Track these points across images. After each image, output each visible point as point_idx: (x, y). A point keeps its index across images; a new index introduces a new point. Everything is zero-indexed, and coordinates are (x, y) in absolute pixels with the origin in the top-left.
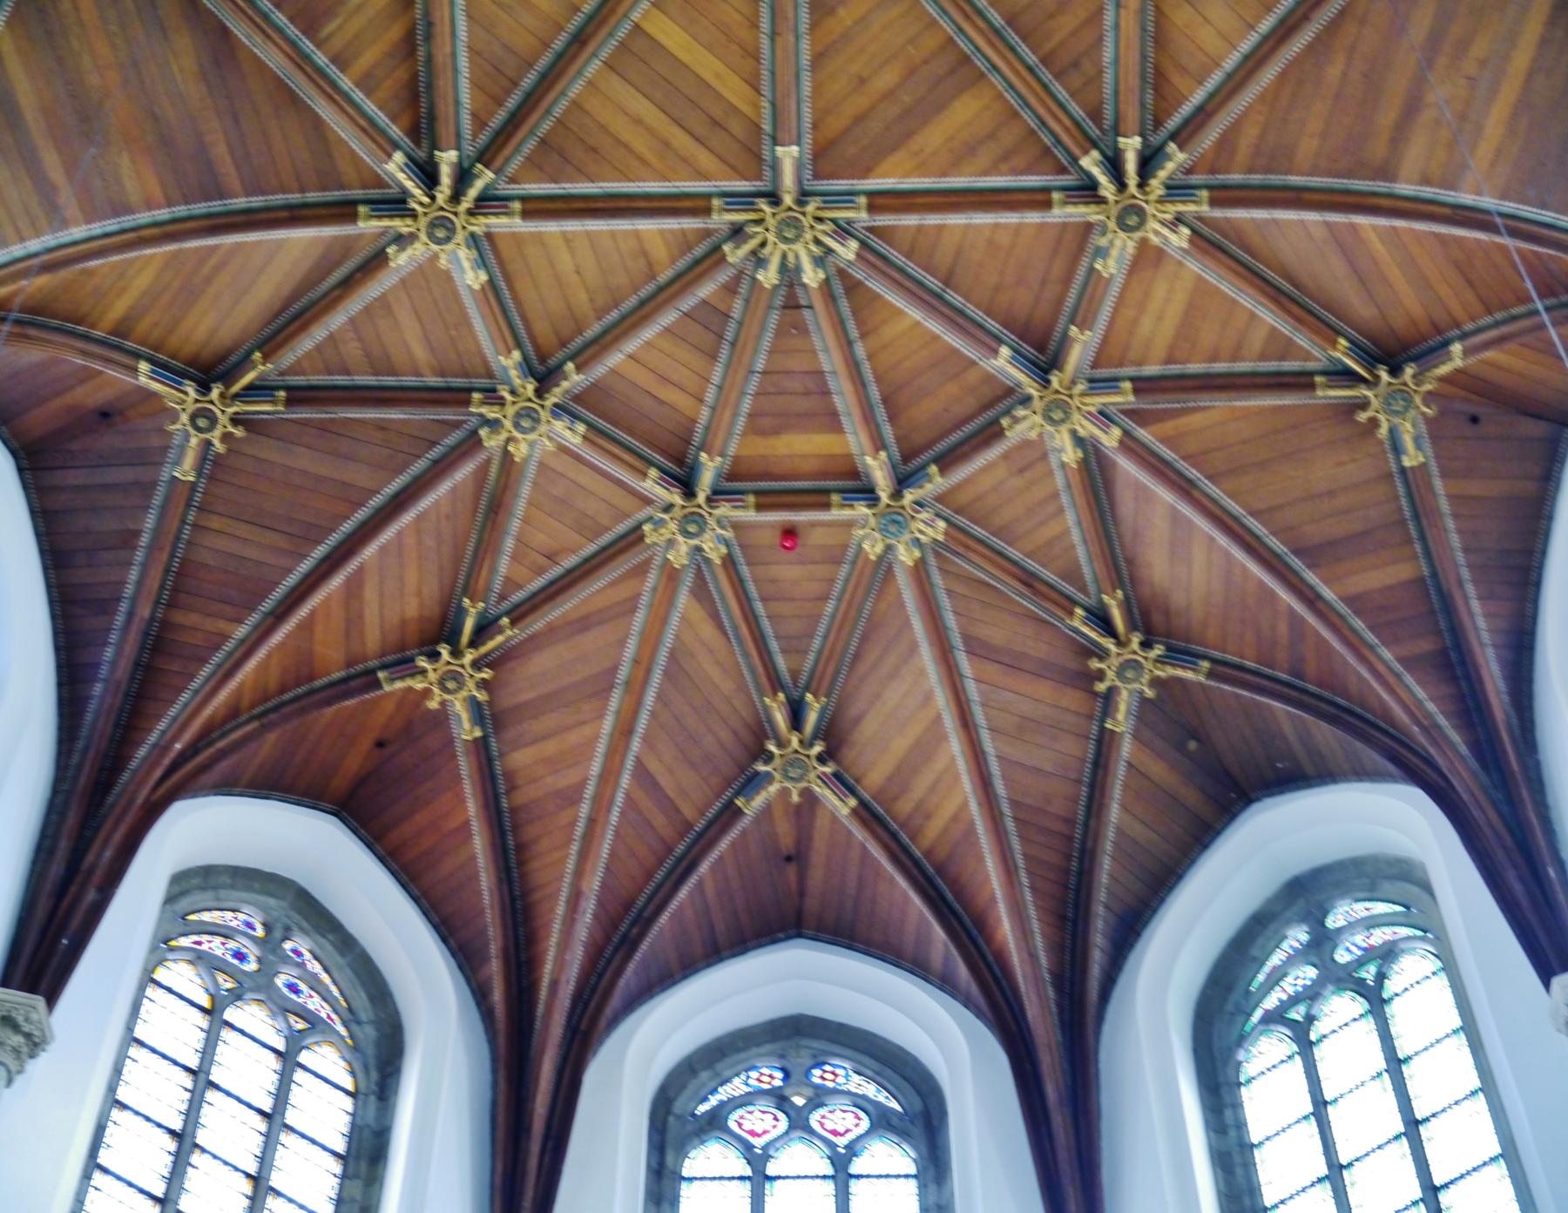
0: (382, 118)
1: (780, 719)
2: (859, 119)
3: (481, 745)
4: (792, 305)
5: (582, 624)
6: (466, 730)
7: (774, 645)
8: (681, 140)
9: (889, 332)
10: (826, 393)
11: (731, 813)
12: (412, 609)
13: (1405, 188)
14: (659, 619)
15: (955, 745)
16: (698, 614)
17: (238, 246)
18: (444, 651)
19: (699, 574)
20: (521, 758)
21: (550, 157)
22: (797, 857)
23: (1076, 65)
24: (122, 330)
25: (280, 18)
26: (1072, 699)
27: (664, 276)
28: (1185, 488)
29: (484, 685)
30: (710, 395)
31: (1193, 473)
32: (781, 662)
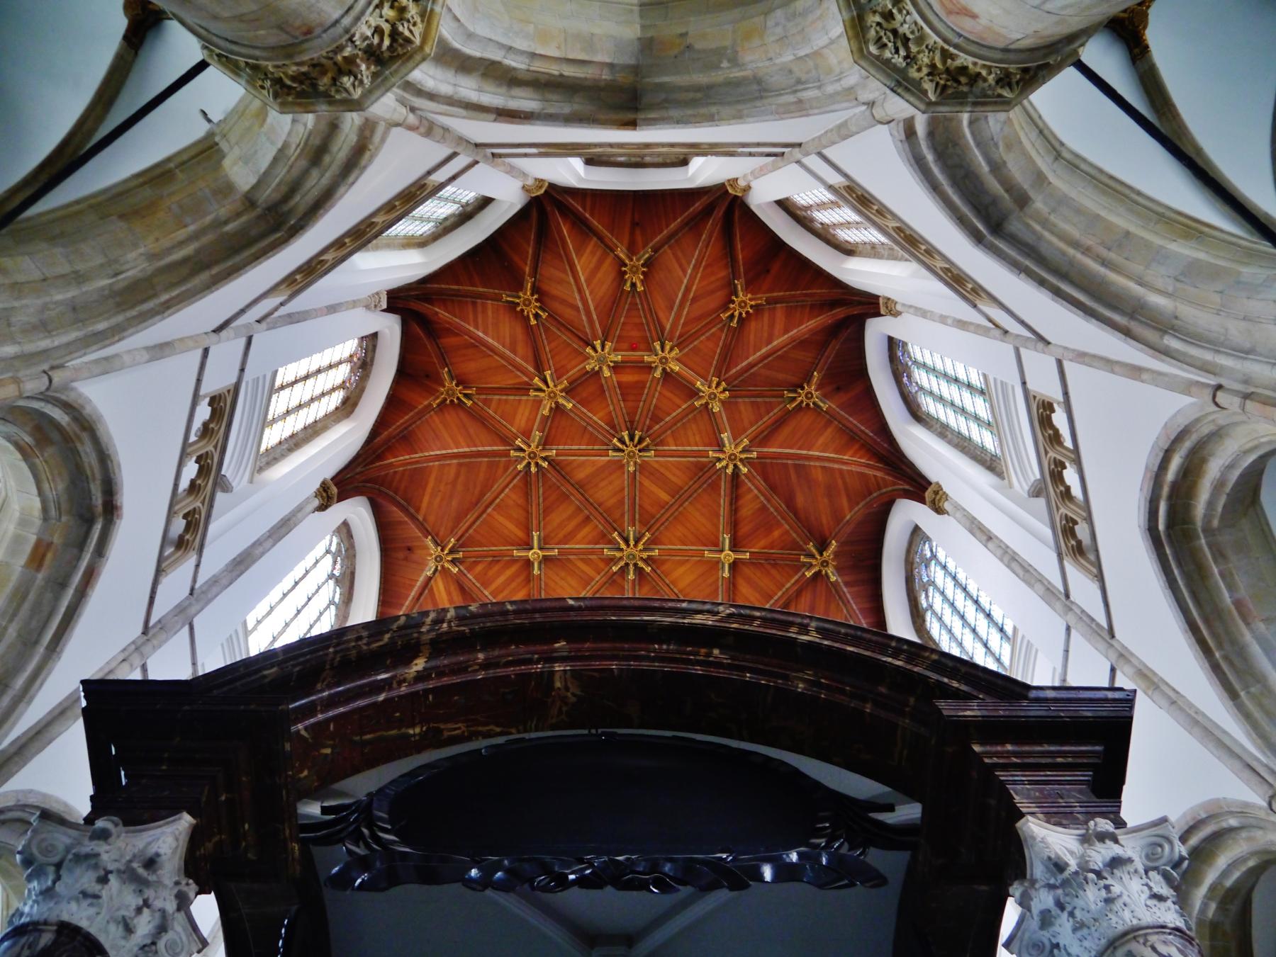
0: (746, 481)
1: (639, 284)
2: (611, 474)
3: (735, 275)
4: (632, 422)
5: (699, 318)
8: (662, 470)
9: (601, 414)
11: (655, 250)
13: (455, 461)
14: (674, 325)
15: (582, 279)
16: (664, 320)
17: (791, 448)
18: (744, 315)
19: (663, 335)
20: (723, 274)
22: (635, 225)
23: (550, 487)
24: (829, 423)
25: (772, 509)
26: (545, 287)
27: (669, 432)
29: (733, 302)
30: (657, 394)
32: (638, 301)
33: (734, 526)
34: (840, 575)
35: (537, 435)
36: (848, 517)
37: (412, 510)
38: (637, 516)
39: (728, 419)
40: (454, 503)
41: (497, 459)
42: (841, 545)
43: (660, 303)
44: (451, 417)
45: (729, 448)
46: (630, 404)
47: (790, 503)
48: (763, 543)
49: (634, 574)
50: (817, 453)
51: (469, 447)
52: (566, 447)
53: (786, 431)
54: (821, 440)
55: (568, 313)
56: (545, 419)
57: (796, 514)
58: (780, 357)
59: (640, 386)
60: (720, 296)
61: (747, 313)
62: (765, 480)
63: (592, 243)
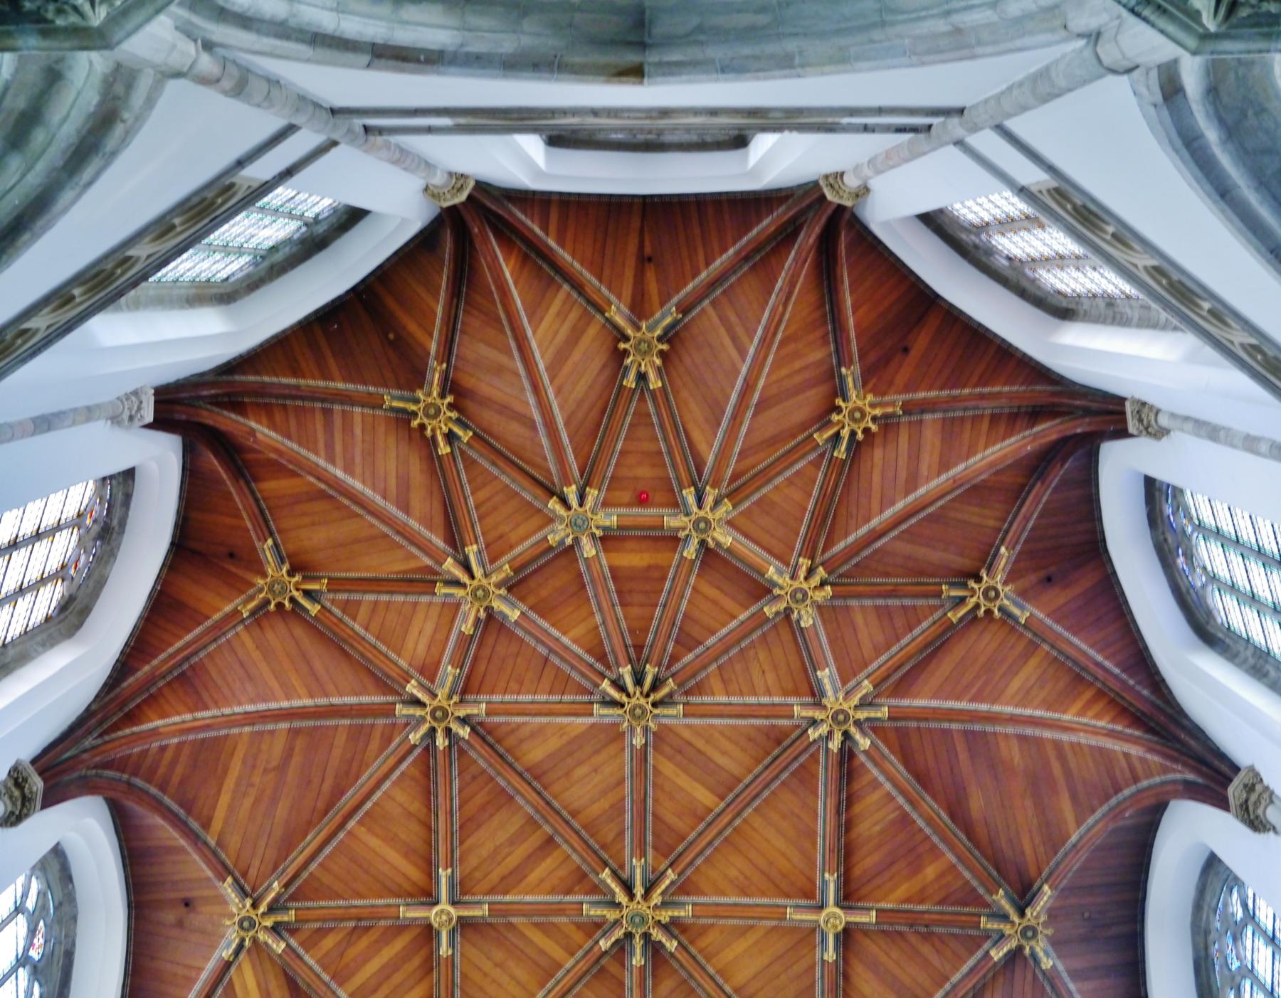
0: (869, 765)
1: (652, 376)
2: (597, 752)
3: (842, 358)
4: (639, 648)
5: (773, 441)
6: (850, 375)
7: (655, 419)
8: (700, 744)
9: (579, 631)
10: (620, 592)
11: (685, 309)
12: (878, 453)
13: (284, 726)
14: (723, 455)
15: (541, 366)
16: (702, 446)
17: (958, 698)
18: (860, 436)
19: (700, 475)
20: (817, 355)
21: (777, 738)
22: (644, 260)
23: (474, 778)
24: (1032, 647)
26: (469, 382)
27: (714, 666)
28: (403, 531)
29: (838, 410)
30: (689, 591)
31: (398, 538)
33: (846, 855)
34: (1059, 957)
35: (449, 672)
36: (1074, 838)
37: (195, 825)
38: (650, 838)
39: (831, 642)
40: (282, 811)
41: (368, 721)
42: (1064, 893)
43: (694, 414)
44: (277, 635)
45: (833, 699)
46: (635, 611)
47: (958, 812)
48: (902, 891)
49: (644, 954)
50: (1008, 709)
51: (311, 696)
52: (508, 698)
53: (944, 667)
54: (1016, 683)
55: (512, 431)
56: (465, 641)
57: (969, 830)
58: (931, 518)
59: (655, 576)
60: (813, 398)
61: (866, 431)
62: (907, 761)
63: (561, 296)
